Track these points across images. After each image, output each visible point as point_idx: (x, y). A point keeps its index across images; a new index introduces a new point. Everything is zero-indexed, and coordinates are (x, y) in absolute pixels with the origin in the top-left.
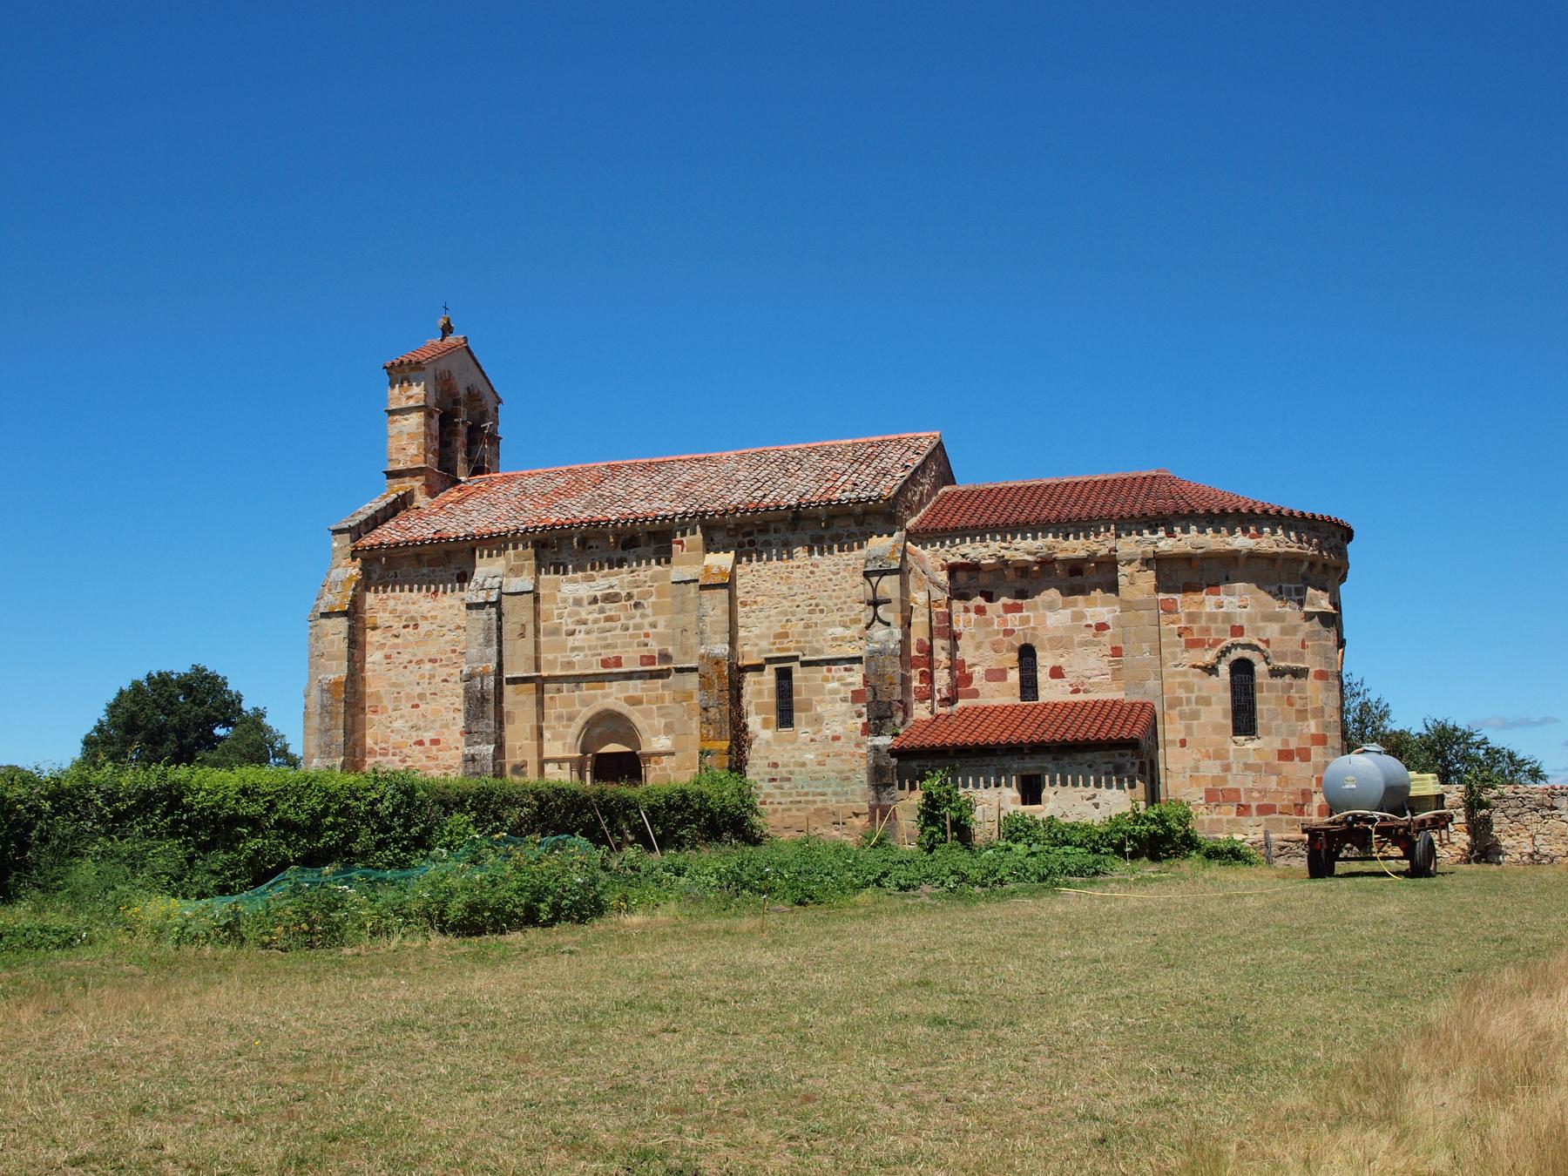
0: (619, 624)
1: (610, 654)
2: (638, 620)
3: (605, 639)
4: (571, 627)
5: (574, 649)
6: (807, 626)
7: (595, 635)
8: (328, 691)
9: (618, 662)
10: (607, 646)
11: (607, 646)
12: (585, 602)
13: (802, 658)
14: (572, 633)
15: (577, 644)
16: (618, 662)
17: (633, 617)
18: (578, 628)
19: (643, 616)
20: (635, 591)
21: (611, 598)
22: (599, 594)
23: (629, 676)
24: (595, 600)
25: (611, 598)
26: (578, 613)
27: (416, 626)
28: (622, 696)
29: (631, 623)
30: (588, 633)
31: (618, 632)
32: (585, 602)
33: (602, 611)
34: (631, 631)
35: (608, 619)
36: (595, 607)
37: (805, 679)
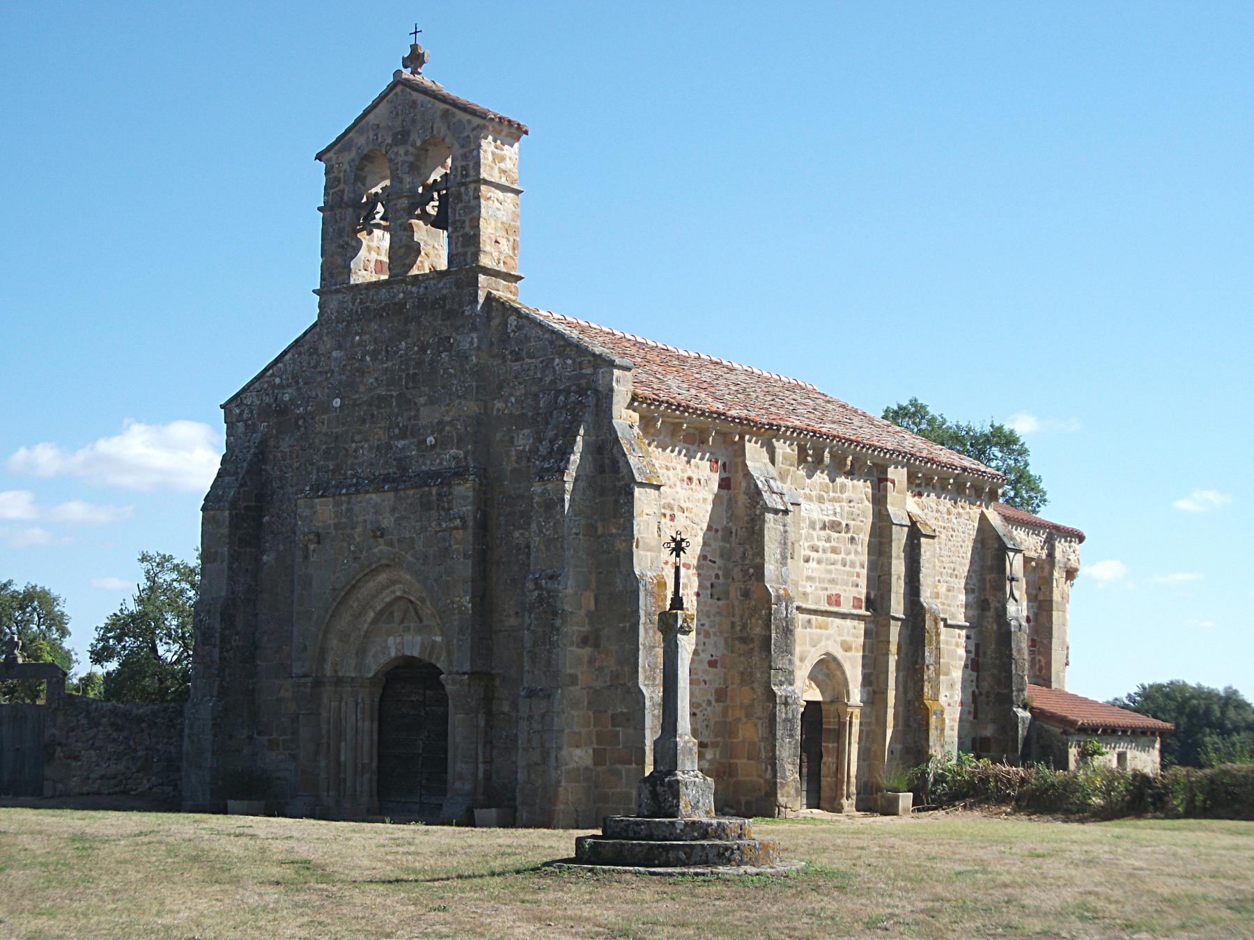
0: (839, 557)
1: (834, 591)
2: (852, 556)
3: (830, 572)
4: (808, 553)
5: (809, 578)
6: (949, 590)
7: (823, 566)
8: (652, 594)
9: (838, 604)
10: (832, 581)
11: (832, 581)
12: (818, 527)
13: (949, 622)
14: (807, 561)
15: (810, 573)
16: (835, 600)
17: (849, 553)
18: (814, 555)
19: (856, 552)
20: (852, 523)
21: (835, 526)
22: (826, 519)
23: (844, 616)
24: (824, 528)
25: (835, 526)
26: (812, 538)
27: (672, 518)
28: (839, 639)
29: (848, 558)
30: (819, 562)
31: (839, 566)
32: (818, 527)
33: (828, 540)
34: (847, 568)
35: (834, 550)
36: (823, 533)
37: (947, 643)
